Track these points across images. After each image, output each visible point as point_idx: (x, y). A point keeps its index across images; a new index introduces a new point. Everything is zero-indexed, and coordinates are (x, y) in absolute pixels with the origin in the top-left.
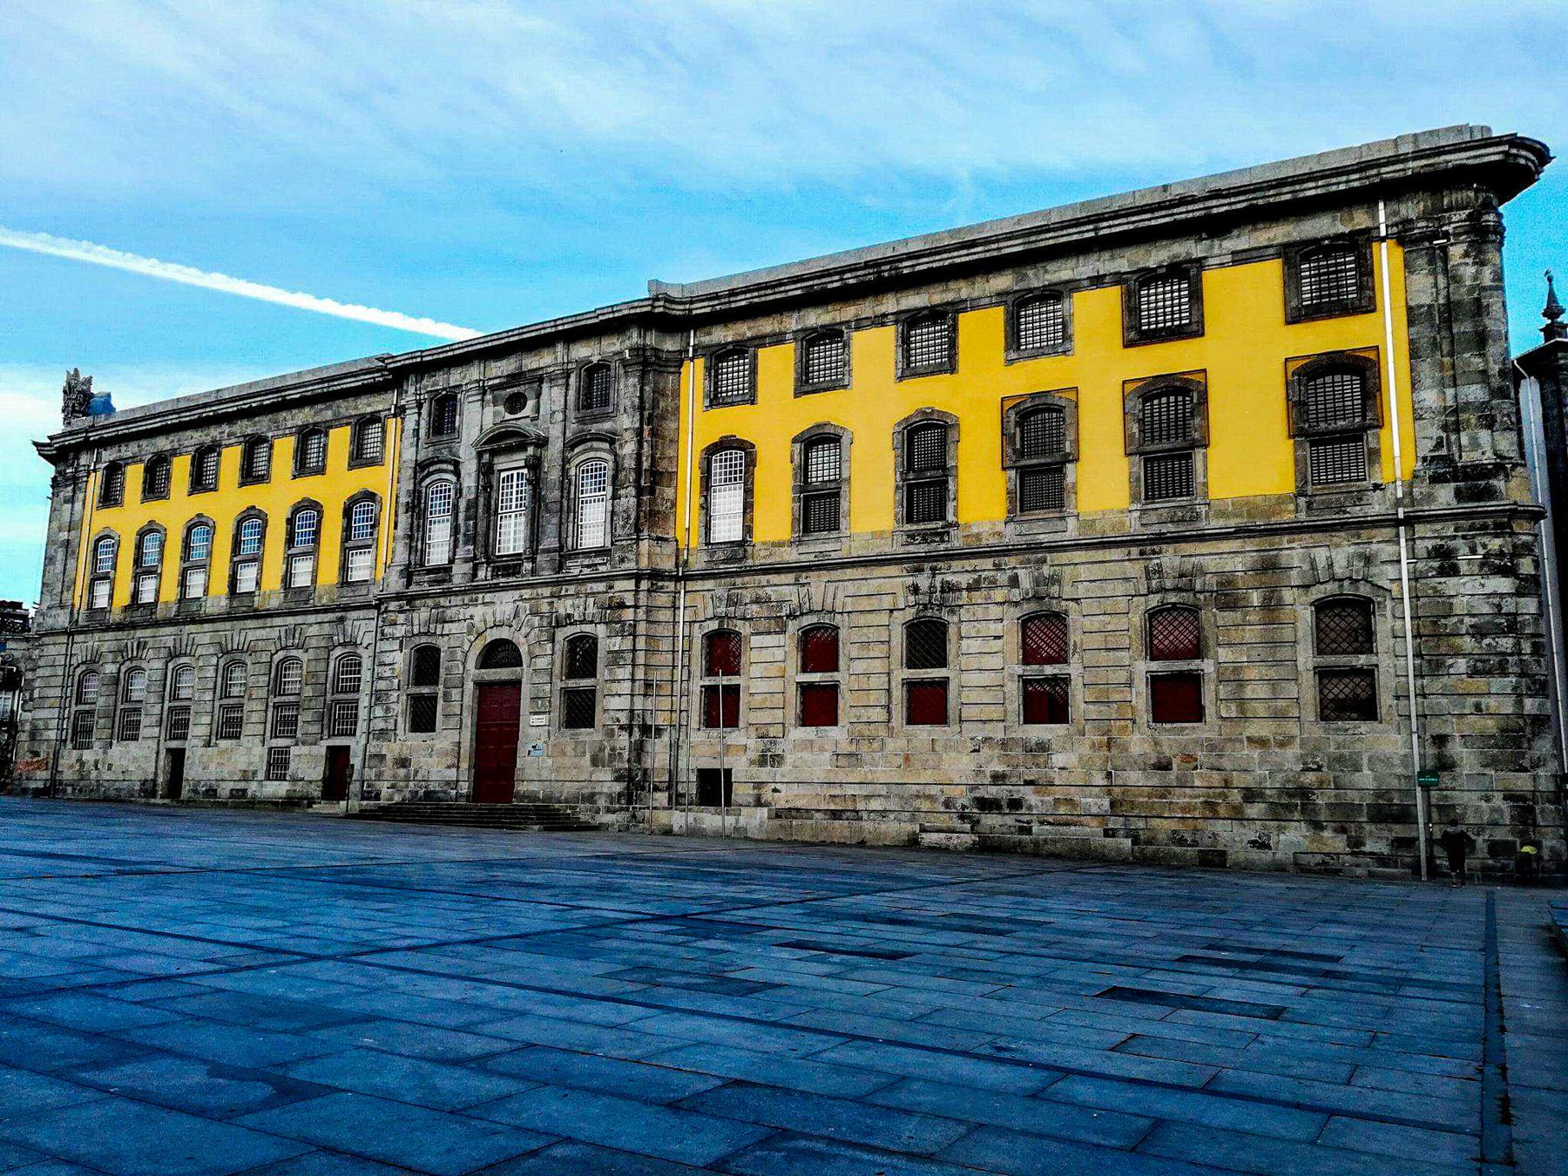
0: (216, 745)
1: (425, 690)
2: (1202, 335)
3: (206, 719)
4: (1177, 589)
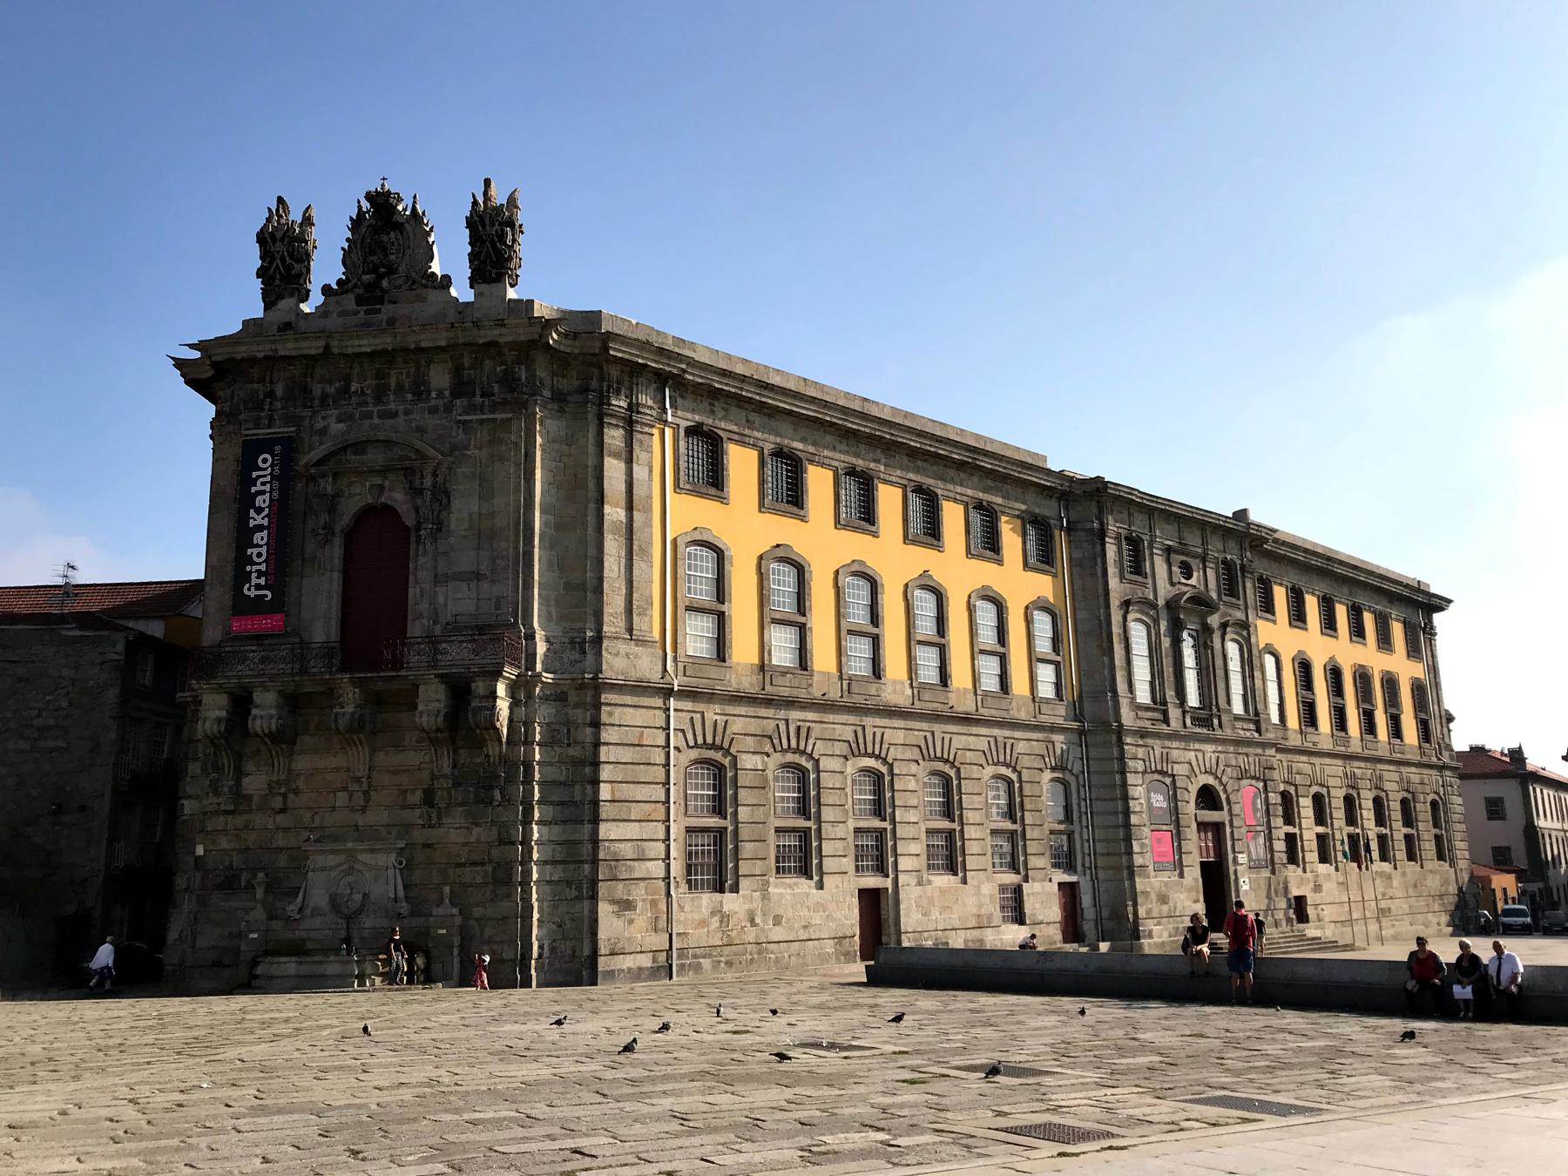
0: (929, 882)
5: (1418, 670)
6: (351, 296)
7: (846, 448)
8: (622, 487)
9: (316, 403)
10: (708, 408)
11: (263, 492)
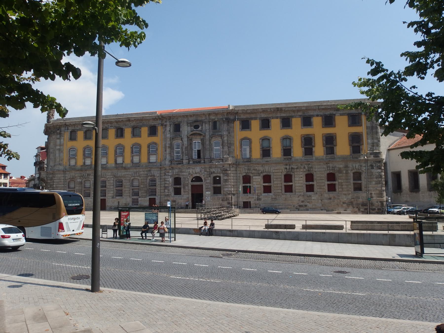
1: (178, 186)
3: (112, 192)
4: (332, 170)
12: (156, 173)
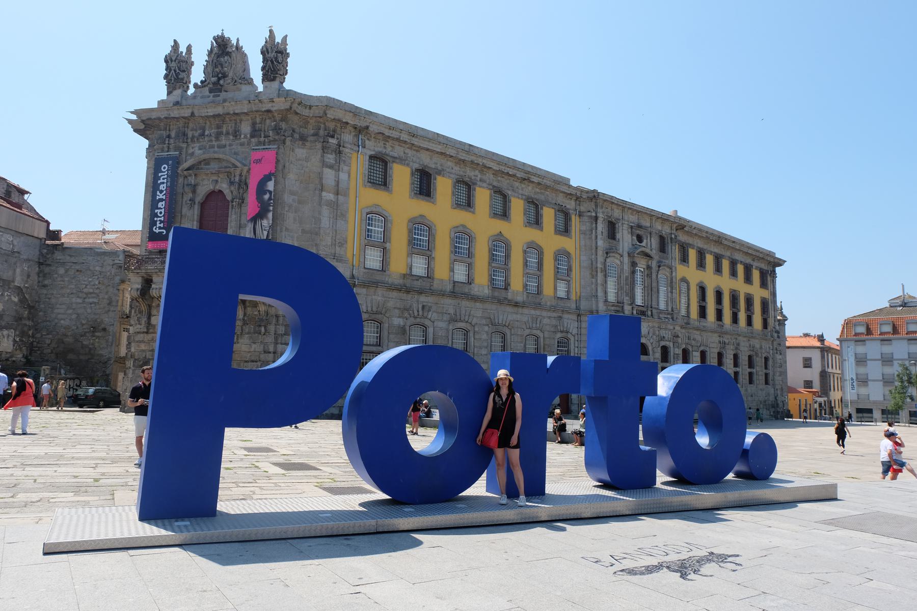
2: (761, 287)
5: (765, 294)
6: (207, 88)
7: (459, 169)
8: (333, 183)
9: (189, 140)
10: (383, 145)
11: (163, 183)
12: (570, 323)
